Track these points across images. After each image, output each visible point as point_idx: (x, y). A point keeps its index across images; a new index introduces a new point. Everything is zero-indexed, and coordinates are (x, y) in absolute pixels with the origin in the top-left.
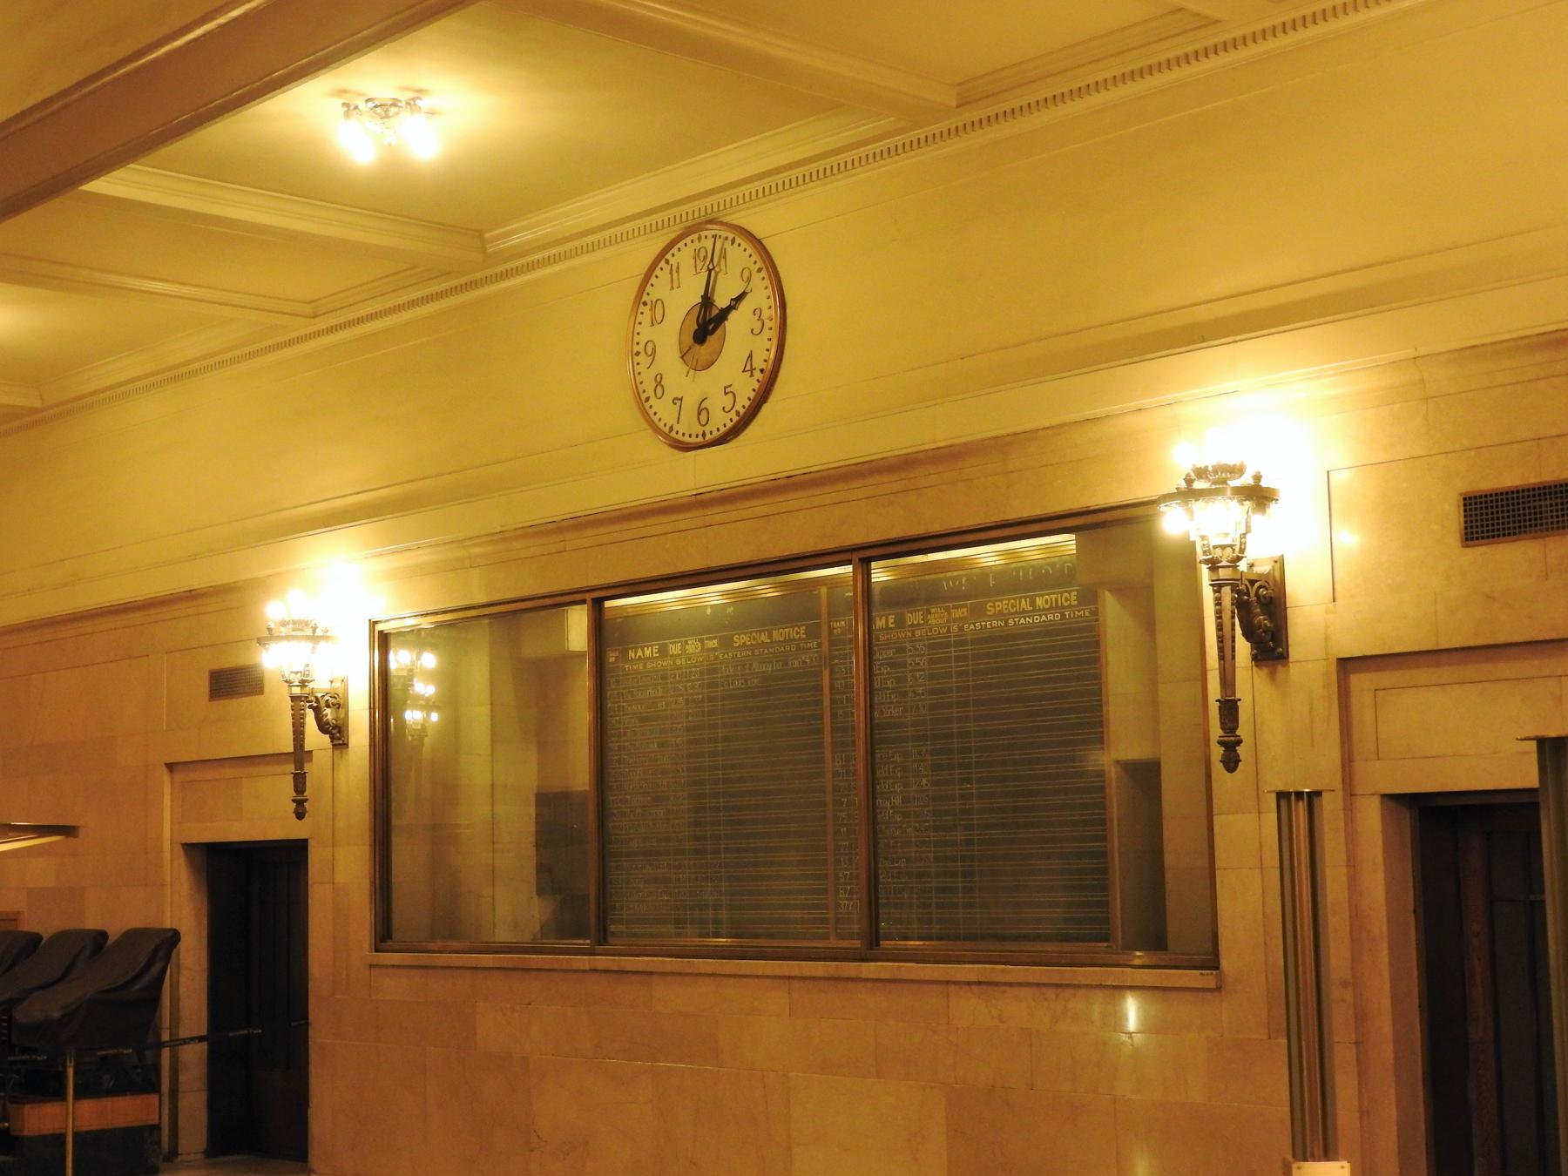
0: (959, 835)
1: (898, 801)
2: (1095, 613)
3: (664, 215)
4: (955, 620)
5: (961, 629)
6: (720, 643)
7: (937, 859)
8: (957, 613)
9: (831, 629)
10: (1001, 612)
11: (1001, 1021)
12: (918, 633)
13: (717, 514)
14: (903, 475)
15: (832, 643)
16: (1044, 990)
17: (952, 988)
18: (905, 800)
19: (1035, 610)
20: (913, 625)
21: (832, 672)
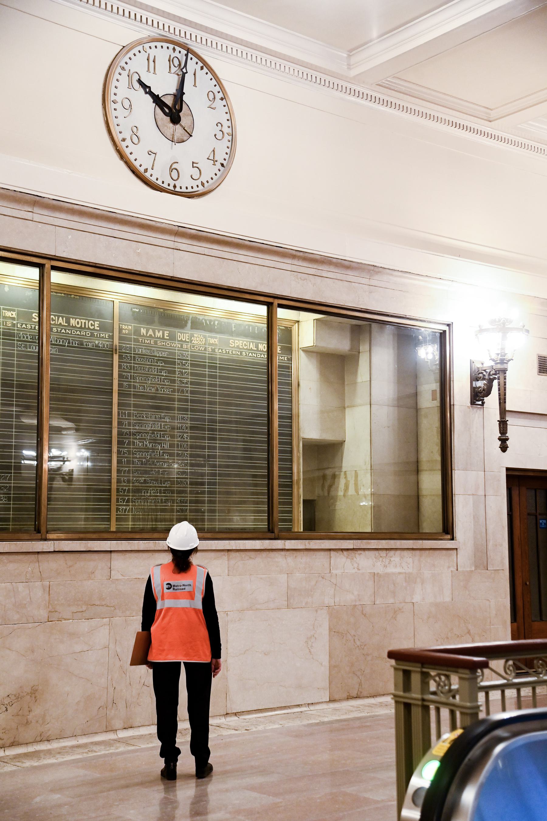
0: (206, 470)
1: (166, 446)
2: (290, 360)
3: (157, 18)
4: (210, 344)
5: (213, 350)
6: (18, 315)
7: (191, 483)
8: (212, 341)
9: (120, 330)
10: (238, 347)
11: (359, 570)
12: (185, 346)
13: (183, 243)
14: (315, 266)
15: (120, 338)
16: (380, 552)
17: (333, 553)
18: (171, 446)
19: (258, 350)
20: (181, 341)
21: (120, 357)
